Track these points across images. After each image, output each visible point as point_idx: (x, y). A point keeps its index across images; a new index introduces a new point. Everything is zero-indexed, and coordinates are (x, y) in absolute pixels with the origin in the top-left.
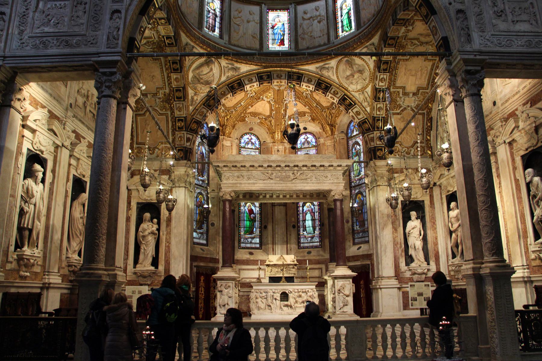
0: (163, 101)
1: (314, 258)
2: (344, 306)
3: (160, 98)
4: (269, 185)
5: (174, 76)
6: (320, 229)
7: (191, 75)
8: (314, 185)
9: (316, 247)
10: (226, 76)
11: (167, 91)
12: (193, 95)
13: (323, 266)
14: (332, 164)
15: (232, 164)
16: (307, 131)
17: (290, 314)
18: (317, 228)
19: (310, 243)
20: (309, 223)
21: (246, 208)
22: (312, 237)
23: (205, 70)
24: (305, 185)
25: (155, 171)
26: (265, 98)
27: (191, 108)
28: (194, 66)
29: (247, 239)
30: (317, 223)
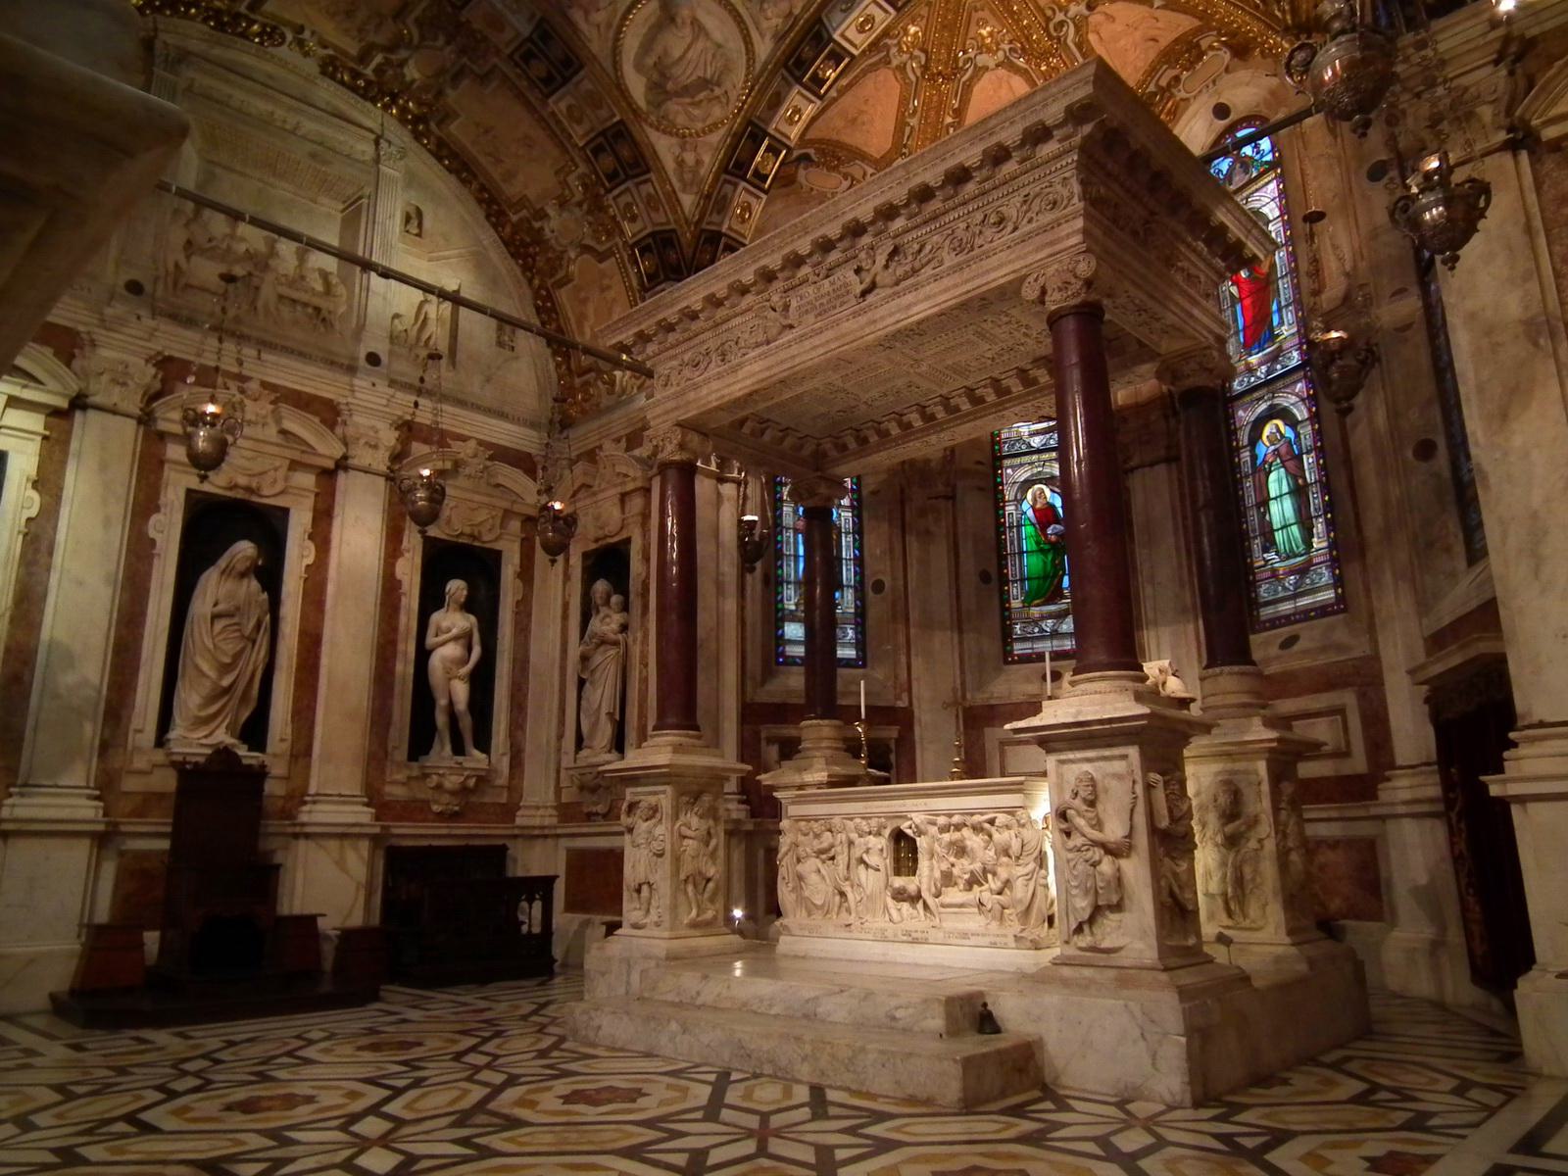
0: (589, 212)
1: (1307, 662)
2: (1097, 911)
3: (579, 204)
4: (783, 355)
5: (560, 104)
6: (1330, 525)
7: (637, 86)
8: (947, 282)
9: (1323, 611)
10: (768, 37)
11: (582, 169)
12: (677, 151)
13: (1348, 698)
14: (994, 140)
15: (653, 321)
16: (1233, 117)
17: (915, 941)
18: (1319, 527)
19: (1295, 596)
20: (1281, 510)
21: (1025, 506)
22: (1303, 571)
23: (675, 43)
24: (909, 298)
25: (618, 440)
26: (983, 59)
27: (688, 201)
28: (631, 44)
29: (1036, 622)
30: (1316, 499)
